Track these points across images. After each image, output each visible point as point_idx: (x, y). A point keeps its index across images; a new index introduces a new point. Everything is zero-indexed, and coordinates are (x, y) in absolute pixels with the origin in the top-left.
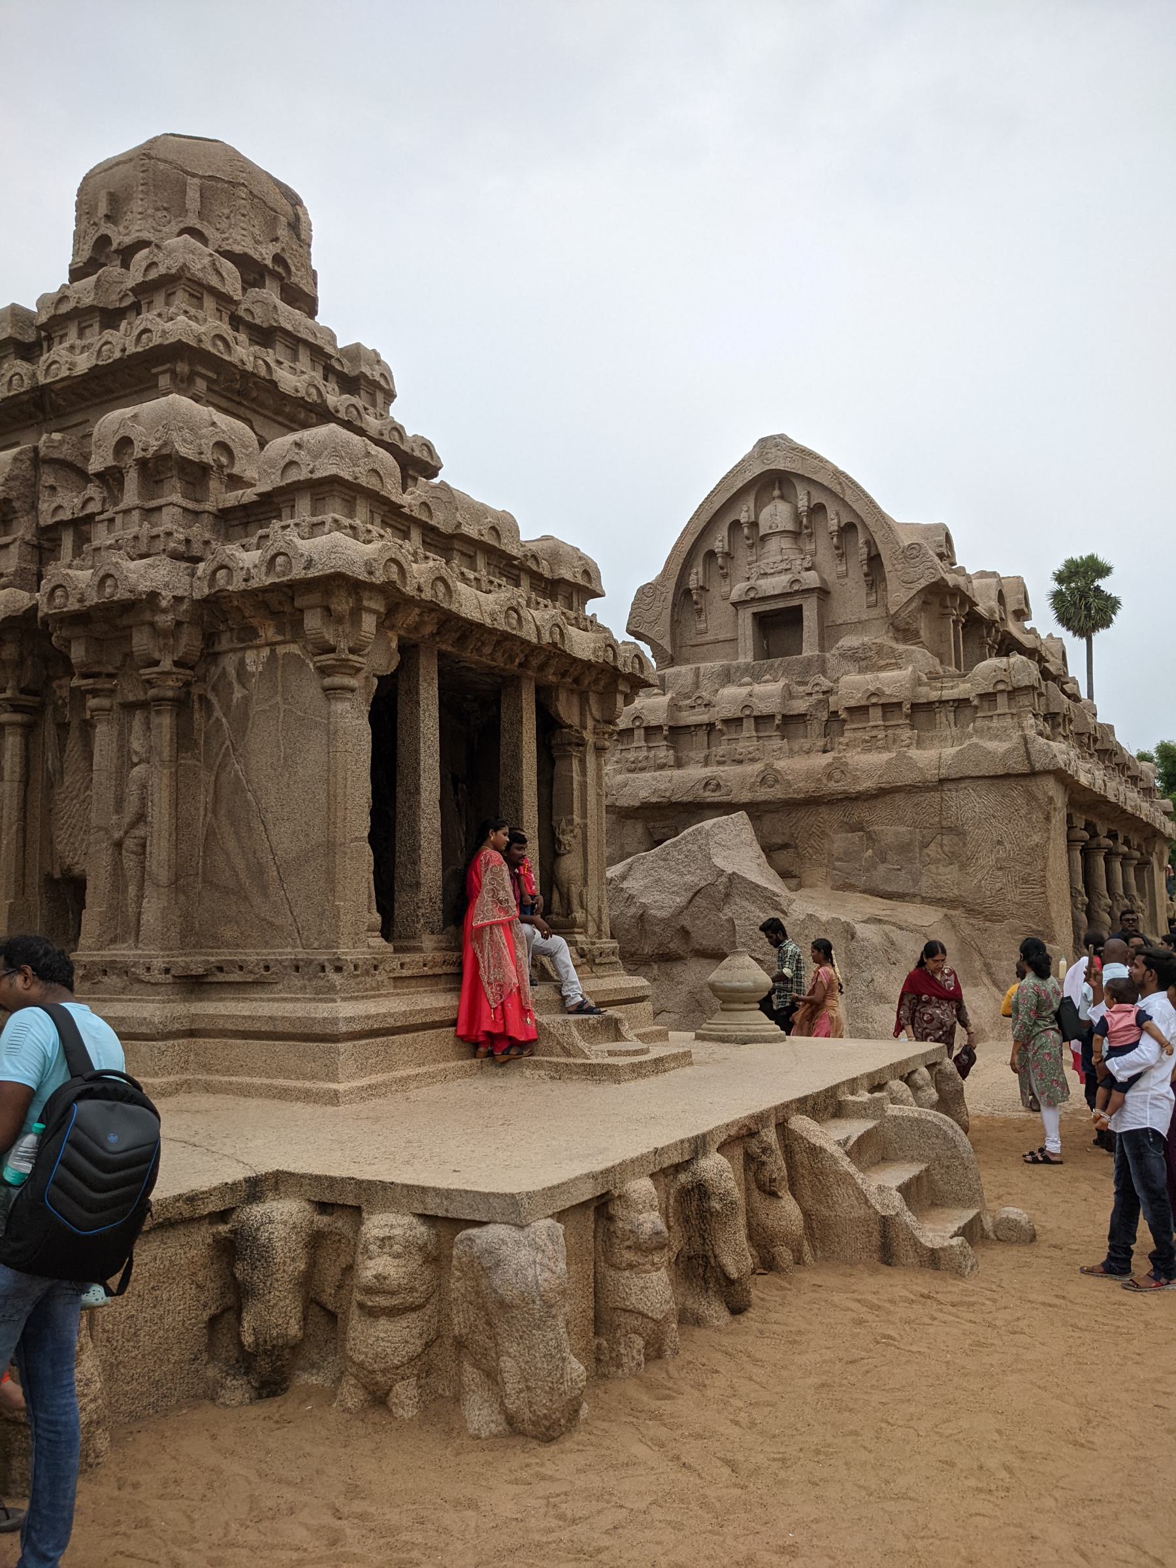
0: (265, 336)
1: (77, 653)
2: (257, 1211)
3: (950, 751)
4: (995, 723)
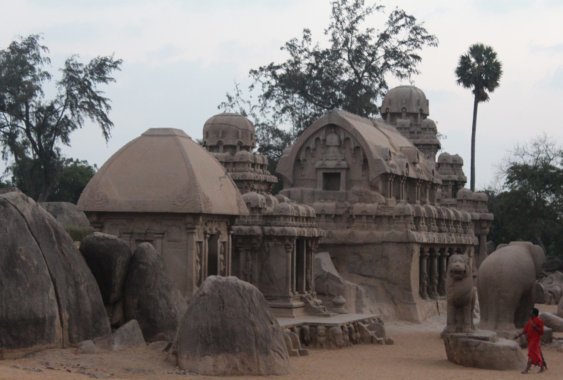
3: (386, 233)
4: (399, 225)
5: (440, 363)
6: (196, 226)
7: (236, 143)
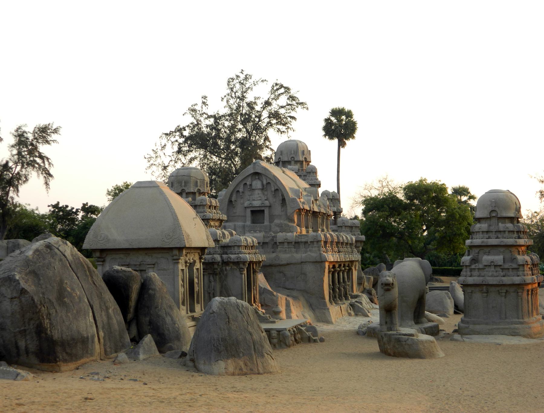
4: (314, 249)
5: (371, 356)
6: (181, 258)
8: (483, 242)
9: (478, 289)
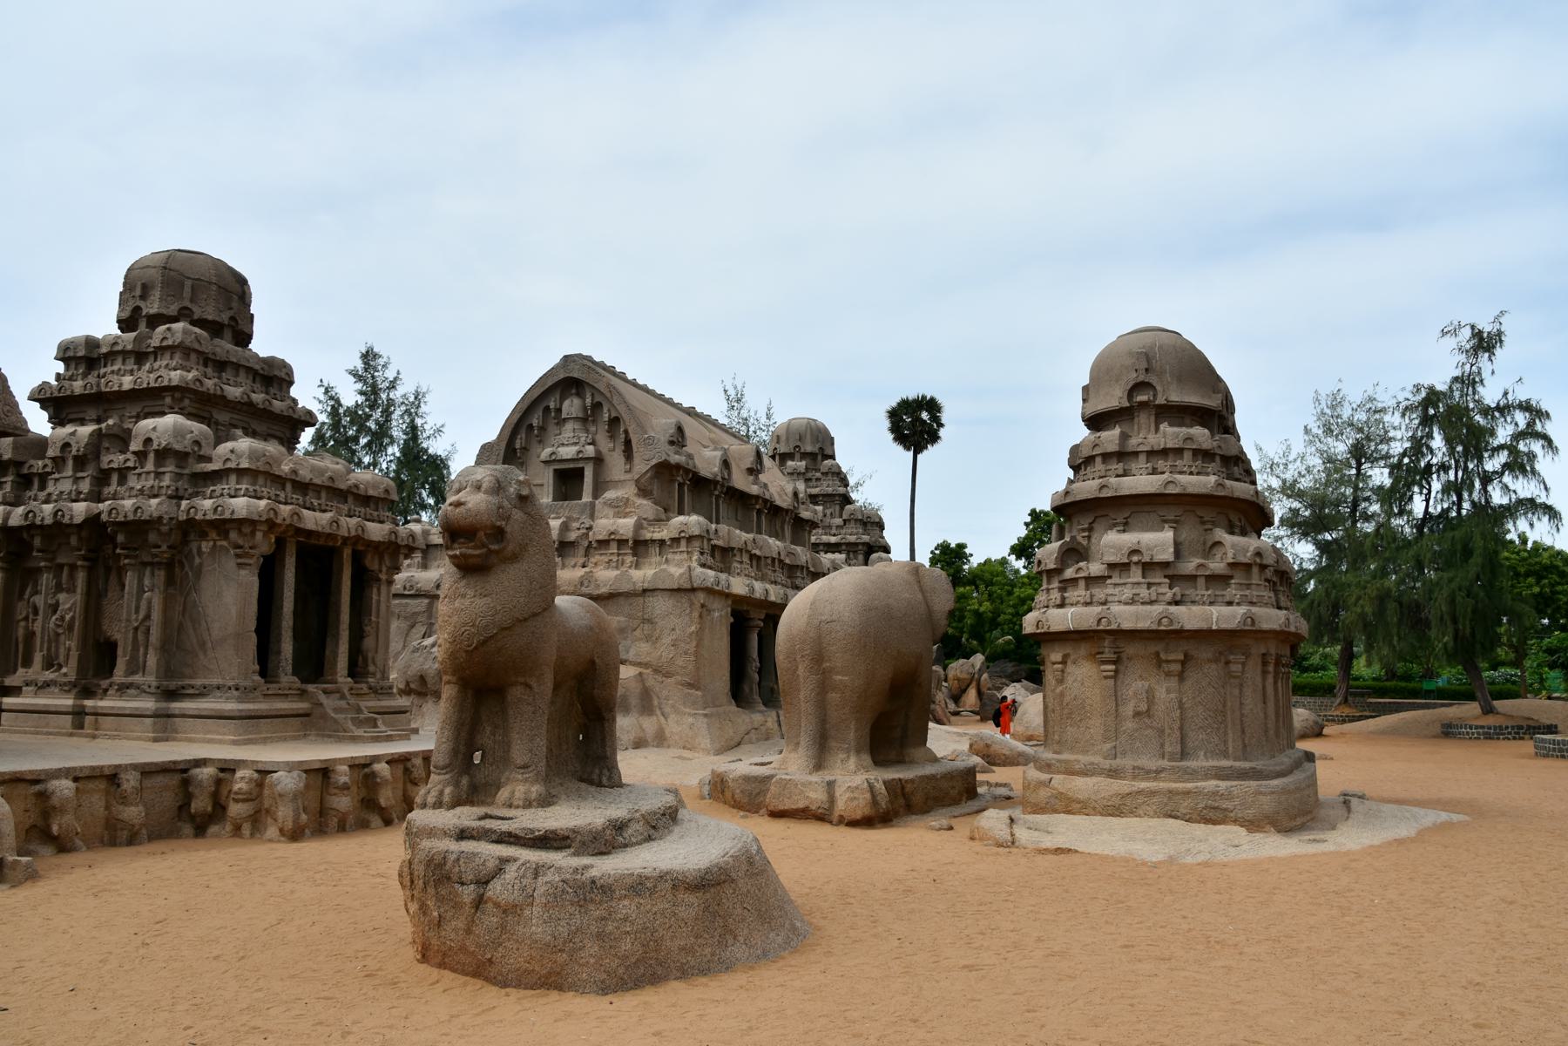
0: (221, 366)
1: (120, 538)
2: (198, 770)
7: (173, 310)
8: (1103, 487)
9: (1084, 649)
